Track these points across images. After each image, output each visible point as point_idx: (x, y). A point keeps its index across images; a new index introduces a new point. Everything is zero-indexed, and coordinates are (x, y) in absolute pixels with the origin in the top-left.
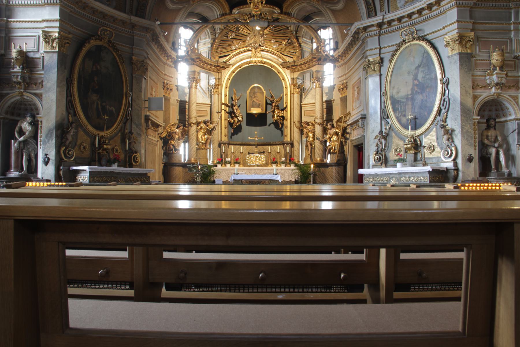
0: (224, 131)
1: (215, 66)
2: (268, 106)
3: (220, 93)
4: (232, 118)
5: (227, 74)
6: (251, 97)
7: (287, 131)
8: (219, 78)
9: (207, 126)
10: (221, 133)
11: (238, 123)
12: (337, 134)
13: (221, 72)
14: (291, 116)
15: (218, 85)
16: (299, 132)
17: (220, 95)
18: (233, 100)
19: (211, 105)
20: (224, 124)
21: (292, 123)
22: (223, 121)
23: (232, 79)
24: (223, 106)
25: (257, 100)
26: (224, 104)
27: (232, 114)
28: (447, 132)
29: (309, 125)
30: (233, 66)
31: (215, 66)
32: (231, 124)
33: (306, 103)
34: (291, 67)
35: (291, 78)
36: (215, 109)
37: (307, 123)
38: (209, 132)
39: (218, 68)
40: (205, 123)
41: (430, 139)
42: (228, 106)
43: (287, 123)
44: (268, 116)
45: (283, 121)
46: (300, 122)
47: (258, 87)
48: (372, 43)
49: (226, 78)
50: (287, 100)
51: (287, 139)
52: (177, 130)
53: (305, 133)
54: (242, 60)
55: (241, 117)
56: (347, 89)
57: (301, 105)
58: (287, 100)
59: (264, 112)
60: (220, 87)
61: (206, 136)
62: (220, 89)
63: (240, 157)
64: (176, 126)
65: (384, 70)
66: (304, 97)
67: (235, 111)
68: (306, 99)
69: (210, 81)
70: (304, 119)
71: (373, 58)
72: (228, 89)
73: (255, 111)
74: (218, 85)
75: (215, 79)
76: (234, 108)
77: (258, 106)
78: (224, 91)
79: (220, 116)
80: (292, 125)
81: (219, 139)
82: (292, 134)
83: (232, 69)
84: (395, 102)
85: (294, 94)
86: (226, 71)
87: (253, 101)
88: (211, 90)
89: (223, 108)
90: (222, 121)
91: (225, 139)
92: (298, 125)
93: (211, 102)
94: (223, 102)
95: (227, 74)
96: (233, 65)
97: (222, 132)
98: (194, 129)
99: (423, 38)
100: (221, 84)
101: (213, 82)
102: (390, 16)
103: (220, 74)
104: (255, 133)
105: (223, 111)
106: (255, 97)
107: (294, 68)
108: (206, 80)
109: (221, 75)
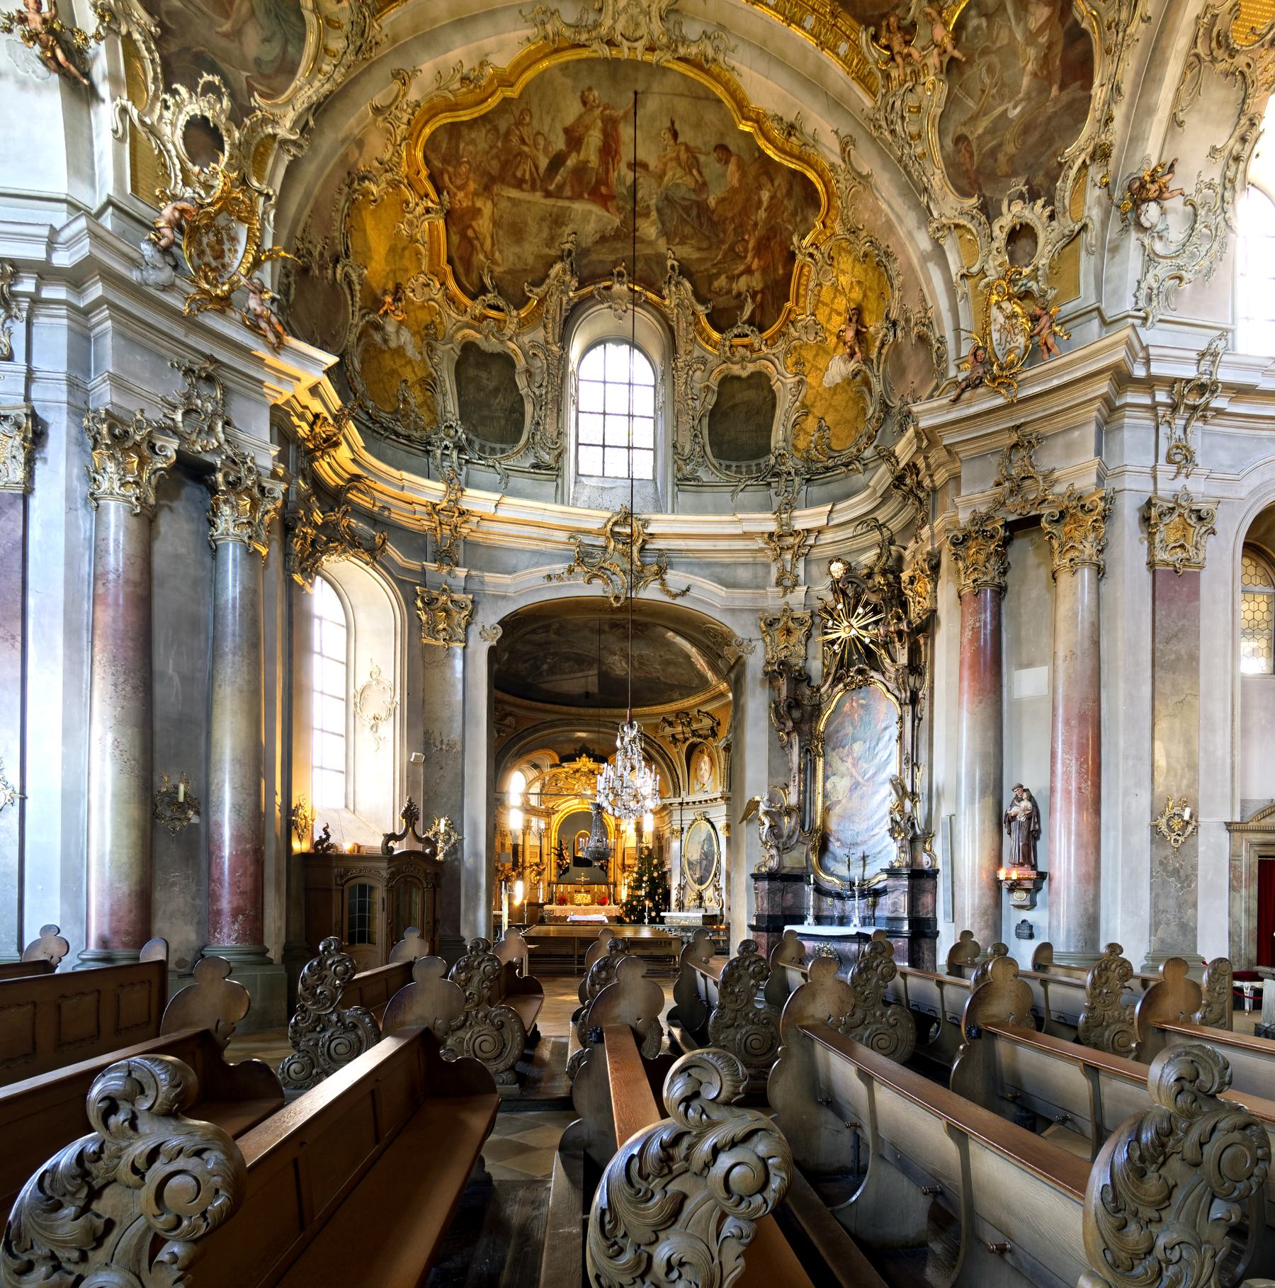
0: (554, 872)
7: (611, 873)
15: (548, 828)
27: (560, 856)
28: (717, 889)
32: (559, 866)
36: (545, 851)
38: (539, 874)
40: (537, 865)
41: (709, 894)
48: (676, 815)
51: (611, 880)
63: (568, 896)
65: (684, 836)
71: (677, 827)
74: (548, 828)
78: (554, 835)
84: (690, 863)
90: (551, 862)
91: (554, 879)
95: (556, 820)
97: (551, 873)
98: (528, 871)
99: (708, 820)
101: (543, 826)
102: (690, 799)
104: (582, 875)
108: (538, 824)
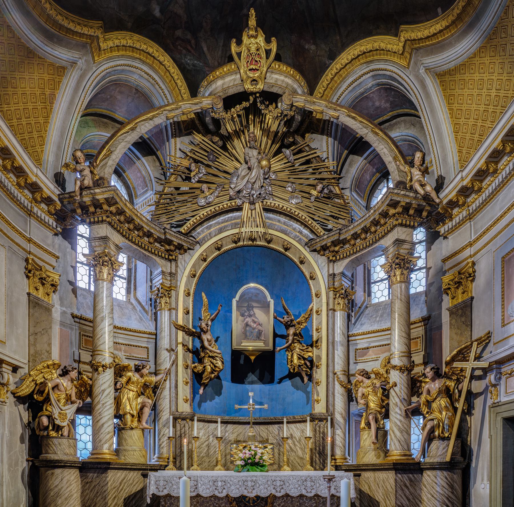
1: (159, 240)
2: (278, 340)
3: (173, 305)
4: (201, 361)
5: (189, 264)
6: (242, 315)
8: (171, 274)
9: (142, 376)
10: (177, 394)
11: (212, 373)
12: (447, 392)
13: (175, 260)
14: (329, 360)
15: (167, 291)
16: (346, 394)
17: (174, 312)
18: (200, 319)
19: (156, 335)
20: (183, 376)
21: (331, 375)
22: (180, 368)
23: (200, 277)
24: (180, 334)
25: (255, 322)
26: (183, 328)
29: (369, 378)
30: (201, 246)
31: (159, 240)
33: (360, 331)
34: (328, 250)
35: (329, 275)
36: (165, 342)
37: (366, 375)
39: (168, 247)
42: (189, 333)
43: (320, 374)
44: (277, 356)
45: (311, 369)
46: (348, 374)
47: (255, 288)
49: (187, 273)
50: (320, 324)
52: (65, 382)
53: (360, 394)
54: (221, 231)
55: (220, 361)
56: (473, 281)
57: (348, 337)
58: (320, 323)
59: (270, 347)
60: (173, 293)
61: (140, 400)
62: (173, 299)
64: (59, 371)
66: (353, 320)
67: (206, 344)
68: (358, 325)
69: (154, 282)
70: (354, 368)
72: (191, 298)
73: (250, 345)
75: (163, 272)
76: (205, 337)
77: (259, 336)
78: (182, 301)
79: (173, 357)
80: (331, 379)
81: (173, 408)
82: (331, 399)
83: (199, 251)
85: (334, 310)
86: (186, 256)
87: (247, 325)
88: (156, 302)
89: (180, 340)
92: (343, 378)
93: (156, 329)
94: (180, 322)
95: (189, 264)
96: (200, 243)
100: (176, 287)
103: (173, 264)
105: (180, 347)
106: (250, 316)
107: (337, 249)
109: (177, 266)
